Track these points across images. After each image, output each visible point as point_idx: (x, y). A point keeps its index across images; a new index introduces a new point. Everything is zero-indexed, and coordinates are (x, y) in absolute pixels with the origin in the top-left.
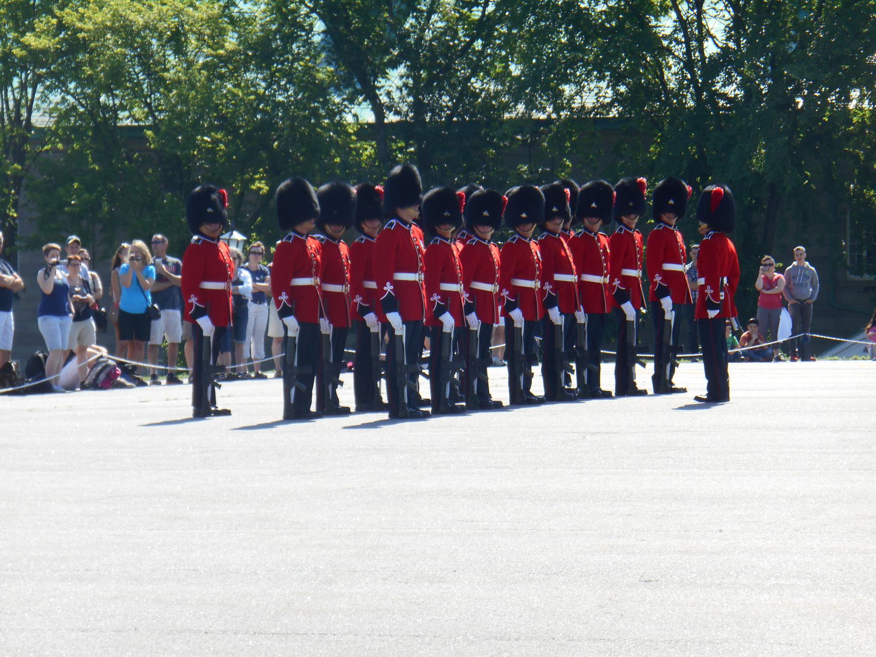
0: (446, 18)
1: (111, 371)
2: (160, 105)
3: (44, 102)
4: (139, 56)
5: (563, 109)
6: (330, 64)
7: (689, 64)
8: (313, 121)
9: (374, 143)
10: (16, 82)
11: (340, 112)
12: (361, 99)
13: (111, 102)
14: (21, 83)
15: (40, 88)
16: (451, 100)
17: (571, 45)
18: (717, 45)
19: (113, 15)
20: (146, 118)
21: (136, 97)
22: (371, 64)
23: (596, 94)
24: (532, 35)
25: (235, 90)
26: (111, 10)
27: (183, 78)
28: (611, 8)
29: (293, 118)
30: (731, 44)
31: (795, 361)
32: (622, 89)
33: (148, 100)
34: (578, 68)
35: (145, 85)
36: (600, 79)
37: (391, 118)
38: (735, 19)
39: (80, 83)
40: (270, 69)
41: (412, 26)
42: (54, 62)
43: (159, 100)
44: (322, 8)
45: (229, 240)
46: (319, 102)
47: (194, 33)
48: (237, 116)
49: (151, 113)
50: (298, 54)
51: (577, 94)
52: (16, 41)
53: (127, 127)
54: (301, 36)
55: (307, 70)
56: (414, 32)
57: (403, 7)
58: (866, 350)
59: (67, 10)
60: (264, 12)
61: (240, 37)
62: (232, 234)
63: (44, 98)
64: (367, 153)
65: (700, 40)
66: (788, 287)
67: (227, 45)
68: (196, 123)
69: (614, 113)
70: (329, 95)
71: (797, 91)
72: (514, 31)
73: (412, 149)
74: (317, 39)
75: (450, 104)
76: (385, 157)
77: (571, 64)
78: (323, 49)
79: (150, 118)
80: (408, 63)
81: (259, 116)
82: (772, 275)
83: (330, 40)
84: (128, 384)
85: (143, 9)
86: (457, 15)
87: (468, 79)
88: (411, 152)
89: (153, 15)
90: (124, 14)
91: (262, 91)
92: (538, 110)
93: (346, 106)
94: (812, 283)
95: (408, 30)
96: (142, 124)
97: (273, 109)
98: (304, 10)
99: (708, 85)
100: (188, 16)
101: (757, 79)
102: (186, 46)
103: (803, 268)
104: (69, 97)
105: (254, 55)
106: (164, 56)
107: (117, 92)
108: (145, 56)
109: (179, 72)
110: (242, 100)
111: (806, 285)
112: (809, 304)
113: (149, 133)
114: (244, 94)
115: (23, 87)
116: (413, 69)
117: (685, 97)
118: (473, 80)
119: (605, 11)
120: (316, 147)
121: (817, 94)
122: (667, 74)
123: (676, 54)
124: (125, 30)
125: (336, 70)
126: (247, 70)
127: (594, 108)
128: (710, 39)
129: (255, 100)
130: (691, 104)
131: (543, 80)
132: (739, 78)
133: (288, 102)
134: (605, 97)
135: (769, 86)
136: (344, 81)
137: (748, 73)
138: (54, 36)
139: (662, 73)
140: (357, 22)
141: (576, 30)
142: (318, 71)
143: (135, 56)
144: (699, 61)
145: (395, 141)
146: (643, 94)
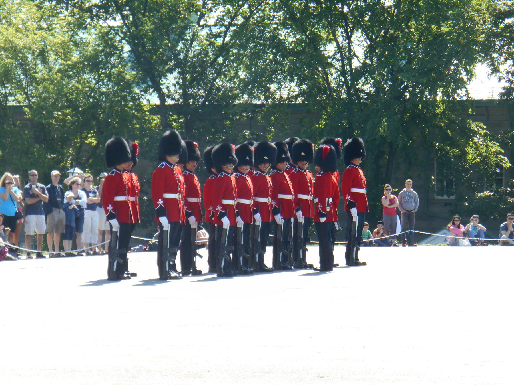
0: (201, 44)
1: (2, 250)
2: (32, 93)
4: (21, 64)
5: (270, 98)
6: (133, 70)
7: (343, 73)
8: (123, 103)
9: (159, 116)
11: (139, 99)
12: (151, 90)
16: (205, 92)
17: (275, 62)
18: (360, 62)
19: (5, 40)
20: (25, 101)
21: (18, 89)
22: (157, 70)
23: (289, 90)
24: (252, 55)
25: (77, 85)
26: (4, 37)
27: (47, 77)
28: (298, 39)
29: (112, 102)
30: (368, 61)
31: (405, 246)
32: (304, 87)
33: (26, 90)
34: (279, 74)
35: (24, 82)
36: (292, 80)
37: (169, 102)
38: (370, 47)
40: (98, 73)
41: (182, 48)
43: (32, 90)
44: (129, 37)
45: (73, 173)
46: (127, 92)
47: (54, 51)
48: (78, 100)
49: (27, 98)
50: (114, 64)
51: (278, 89)
53: (13, 106)
54: (116, 53)
55: (120, 73)
56: (183, 52)
57: (177, 37)
58: (446, 240)
60: (95, 38)
61: (80, 53)
62: (74, 170)
64: (156, 122)
65: (350, 59)
66: (400, 203)
67: (73, 58)
68: (54, 103)
69: (299, 100)
70: (133, 88)
71: (406, 88)
72: (242, 52)
73: (182, 120)
74: (125, 55)
75: (204, 94)
76: (166, 124)
77: (275, 72)
78: (130, 61)
79: (27, 101)
80: (180, 70)
81: (91, 100)
82: (389, 197)
83: (133, 56)
84: (13, 258)
85: (23, 37)
86: (208, 42)
87: (214, 80)
88: (181, 122)
90: (11, 39)
91: (93, 86)
92: (255, 98)
93: (142, 95)
94: (415, 201)
95: (179, 51)
96: (22, 104)
97: (100, 96)
98: (118, 38)
99: (353, 85)
100: (50, 41)
101: (382, 81)
102: (48, 59)
103: (409, 192)
105: (88, 65)
106: (35, 65)
107: (8, 85)
108: (23, 65)
109: (45, 74)
110: (81, 91)
111: (411, 202)
112: (413, 213)
113: (26, 109)
114: (83, 87)
116: (182, 73)
117: (341, 92)
118: (217, 80)
119: (294, 42)
120: (125, 119)
121: (418, 91)
122: (330, 79)
123: (336, 66)
124: (12, 49)
125: (137, 74)
126: (84, 73)
127: (288, 98)
128: (355, 58)
129: (89, 90)
130: (344, 96)
131: (259, 80)
132: (372, 81)
133: (109, 92)
134: (294, 92)
136: (141, 80)
137: (378, 78)
139: (327, 78)
140: (149, 46)
141: (277, 52)
142: (126, 74)
143: (18, 64)
144: (349, 71)
145: (172, 116)
146: (316, 90)
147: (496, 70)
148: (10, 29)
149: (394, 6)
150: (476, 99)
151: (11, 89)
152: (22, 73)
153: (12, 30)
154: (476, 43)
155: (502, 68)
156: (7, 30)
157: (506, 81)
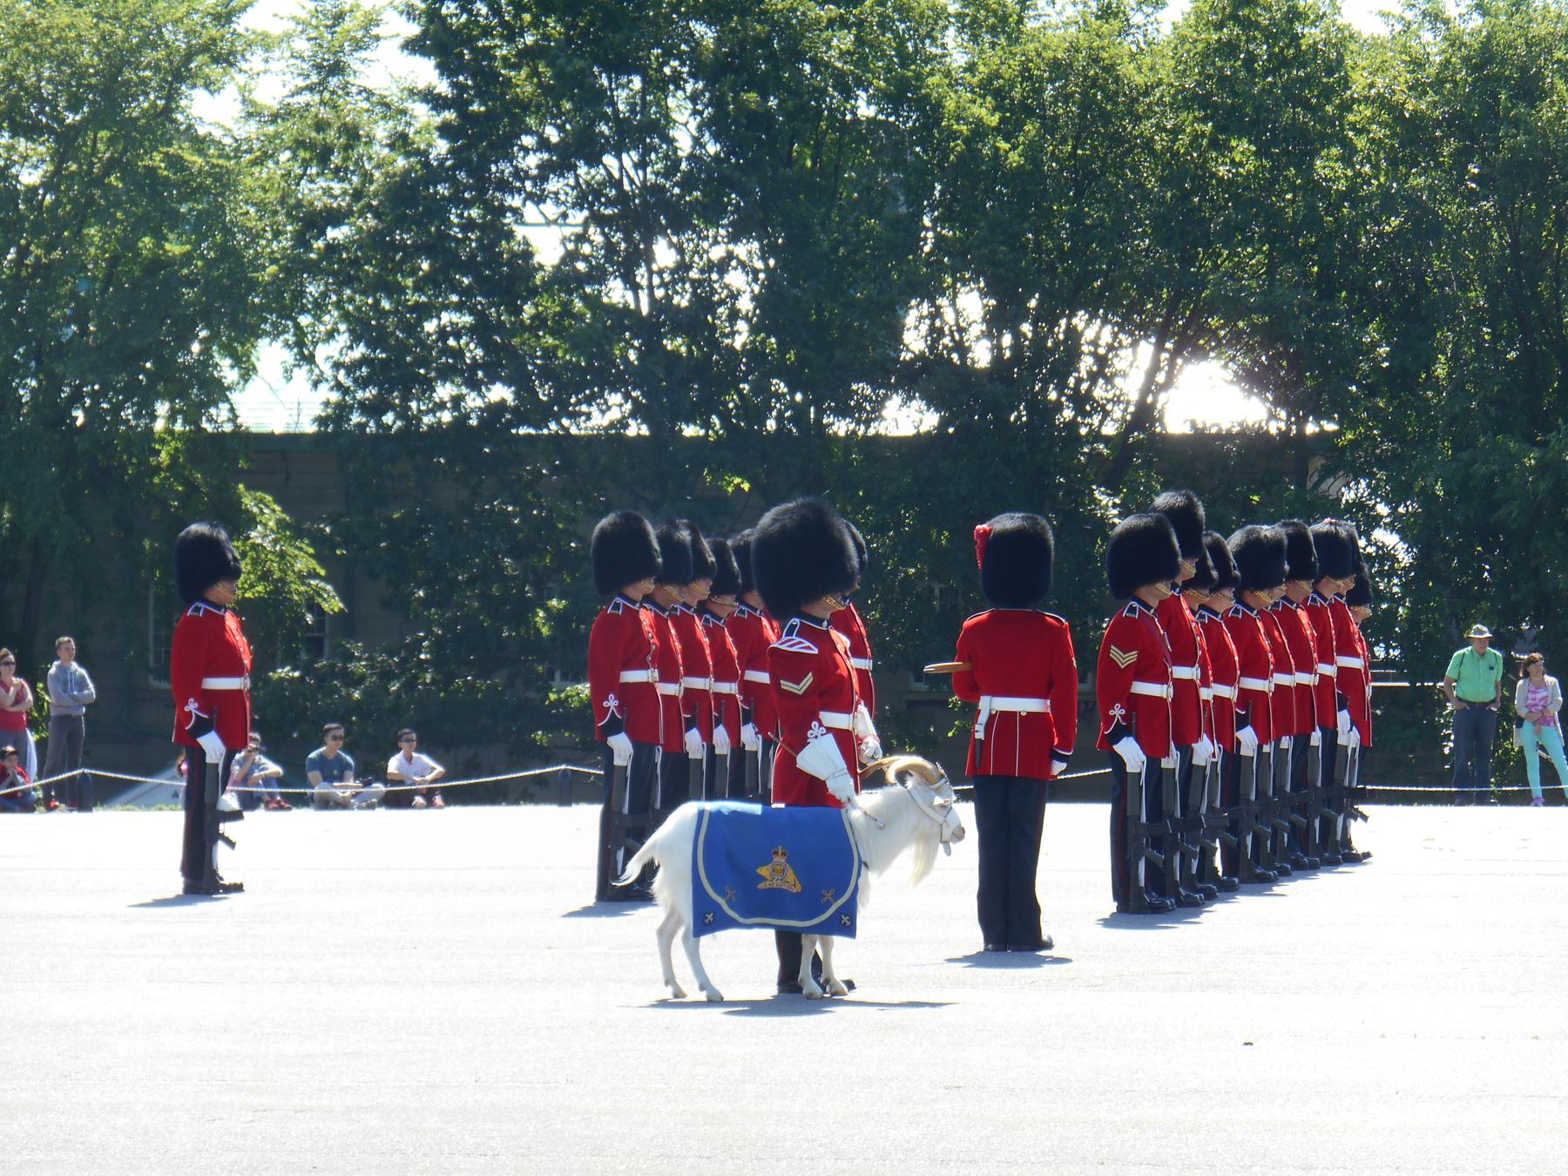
58: (176, 795)
71: (76, 398)
121: (105, 406)
135: (33, 391)
147: (310, 359)
149: (43, 184)
150: (254, 430)
154: (253, 285)
155: (325, 353)
157: (332, 389)
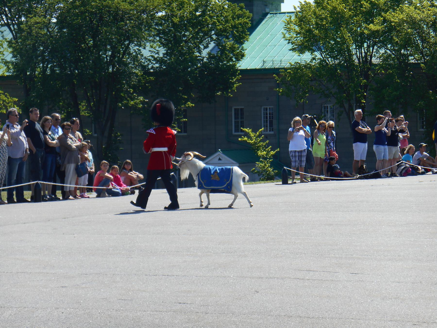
3: (377, 53)
10: (365, 45)
13: (406, 53)
14: (368, 45)
15: (375, 47)
39: (393, 45)
42: (382, 36)
52: (366, 28)
59: (388, 13)
63: (377, 52)
89: (423, 15)
96: (419, 62)
104: (388, 51)
113: (422, 65)
115: (368, 47)
138: (382, 25)
143: (416, 33)
148: (411, 7)
151: (411, 51)
152: (419, 39)
153: (412, 8)
156: (409, 8)
